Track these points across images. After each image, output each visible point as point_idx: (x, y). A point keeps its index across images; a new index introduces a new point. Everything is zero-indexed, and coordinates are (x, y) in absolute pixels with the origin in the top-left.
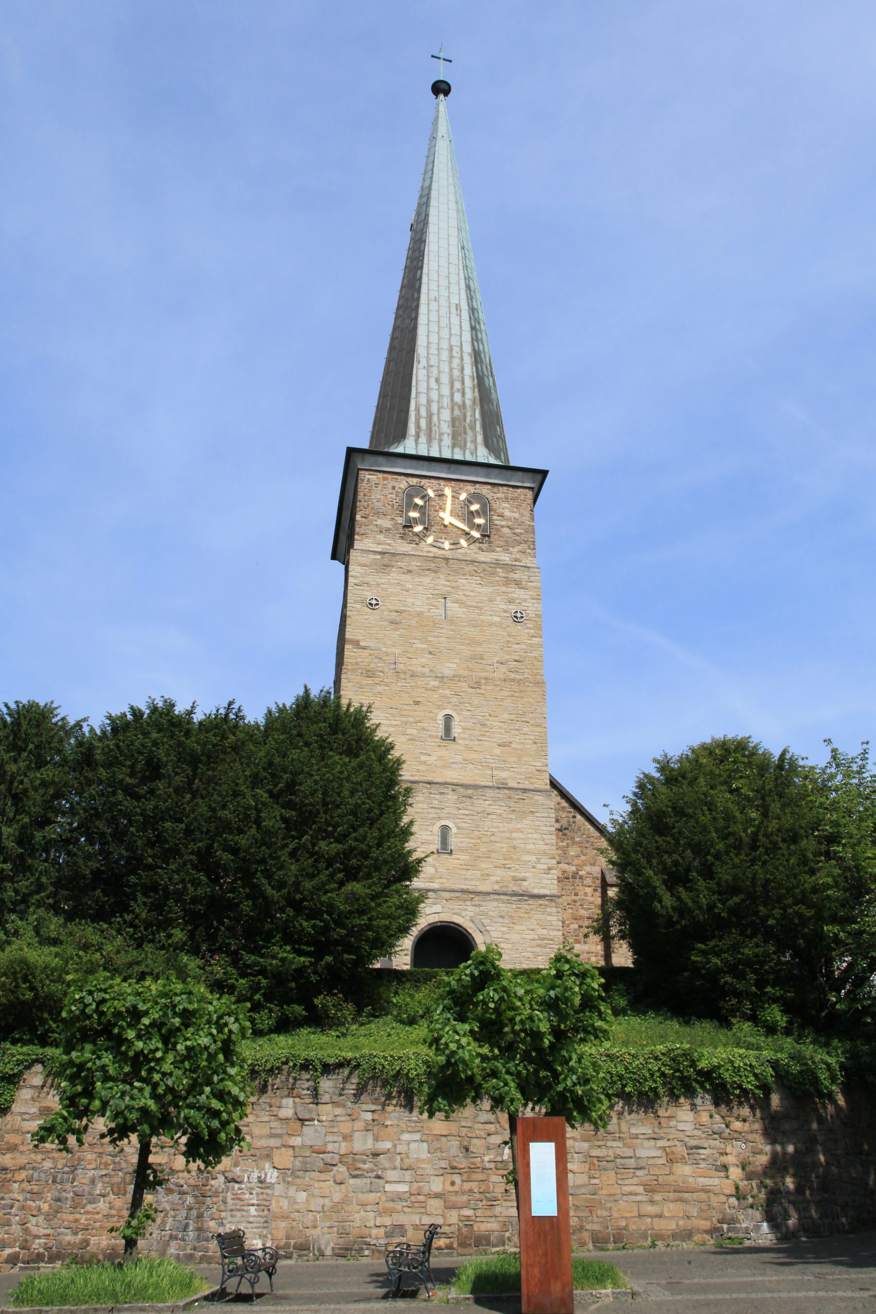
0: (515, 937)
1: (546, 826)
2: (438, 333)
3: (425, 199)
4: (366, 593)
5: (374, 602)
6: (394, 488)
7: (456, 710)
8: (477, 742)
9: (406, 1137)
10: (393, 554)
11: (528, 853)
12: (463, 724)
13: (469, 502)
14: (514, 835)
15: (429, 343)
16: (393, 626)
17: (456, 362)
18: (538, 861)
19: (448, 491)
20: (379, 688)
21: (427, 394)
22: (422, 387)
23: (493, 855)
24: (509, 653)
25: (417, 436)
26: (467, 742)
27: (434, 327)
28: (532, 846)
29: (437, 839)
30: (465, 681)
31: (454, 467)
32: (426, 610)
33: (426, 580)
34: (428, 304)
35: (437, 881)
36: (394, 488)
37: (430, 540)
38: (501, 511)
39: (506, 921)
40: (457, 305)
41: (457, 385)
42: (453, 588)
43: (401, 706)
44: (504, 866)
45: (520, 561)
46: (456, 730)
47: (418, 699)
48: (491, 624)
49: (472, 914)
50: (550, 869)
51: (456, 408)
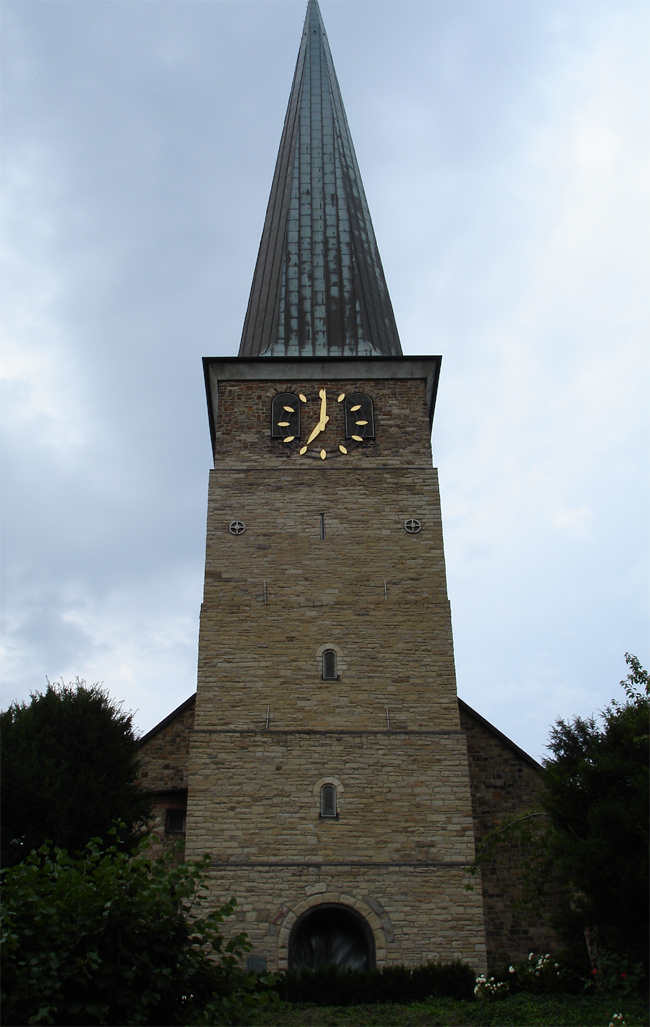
0: (423, 919)
1: (458, 776)
4: (228, 518)
6: (259, 397)
7: (339, 644)
8: (366, 680)
12: (348, 659)
13: (348, 403)
14: (418, 790)
15: (300, 238)
16: (261, 553)
17: (332, 254)
18: (449, 821)
19: (323, 394)
20: (245, 626)
21: (299, 292)
23: (391, 817)
26: (354, 681)
28: (441, 803)
29: (318, 801)
30: (350, 608)
31: (328, 366)
32: (300, 530)
33: (300, 496)
35: (322, 853)
36: (259, 397)
37: (303, 450)
38: (389, 409)
39: (411, 899)
40: (332, 195)
41: (334, 278)
42: (332, 501)
43: (271, 644)
44: (405, 830)
45: (413, 464)
46: (340, 668)
47: (292, 634)
49: (365, 892)
50: (465, 830)
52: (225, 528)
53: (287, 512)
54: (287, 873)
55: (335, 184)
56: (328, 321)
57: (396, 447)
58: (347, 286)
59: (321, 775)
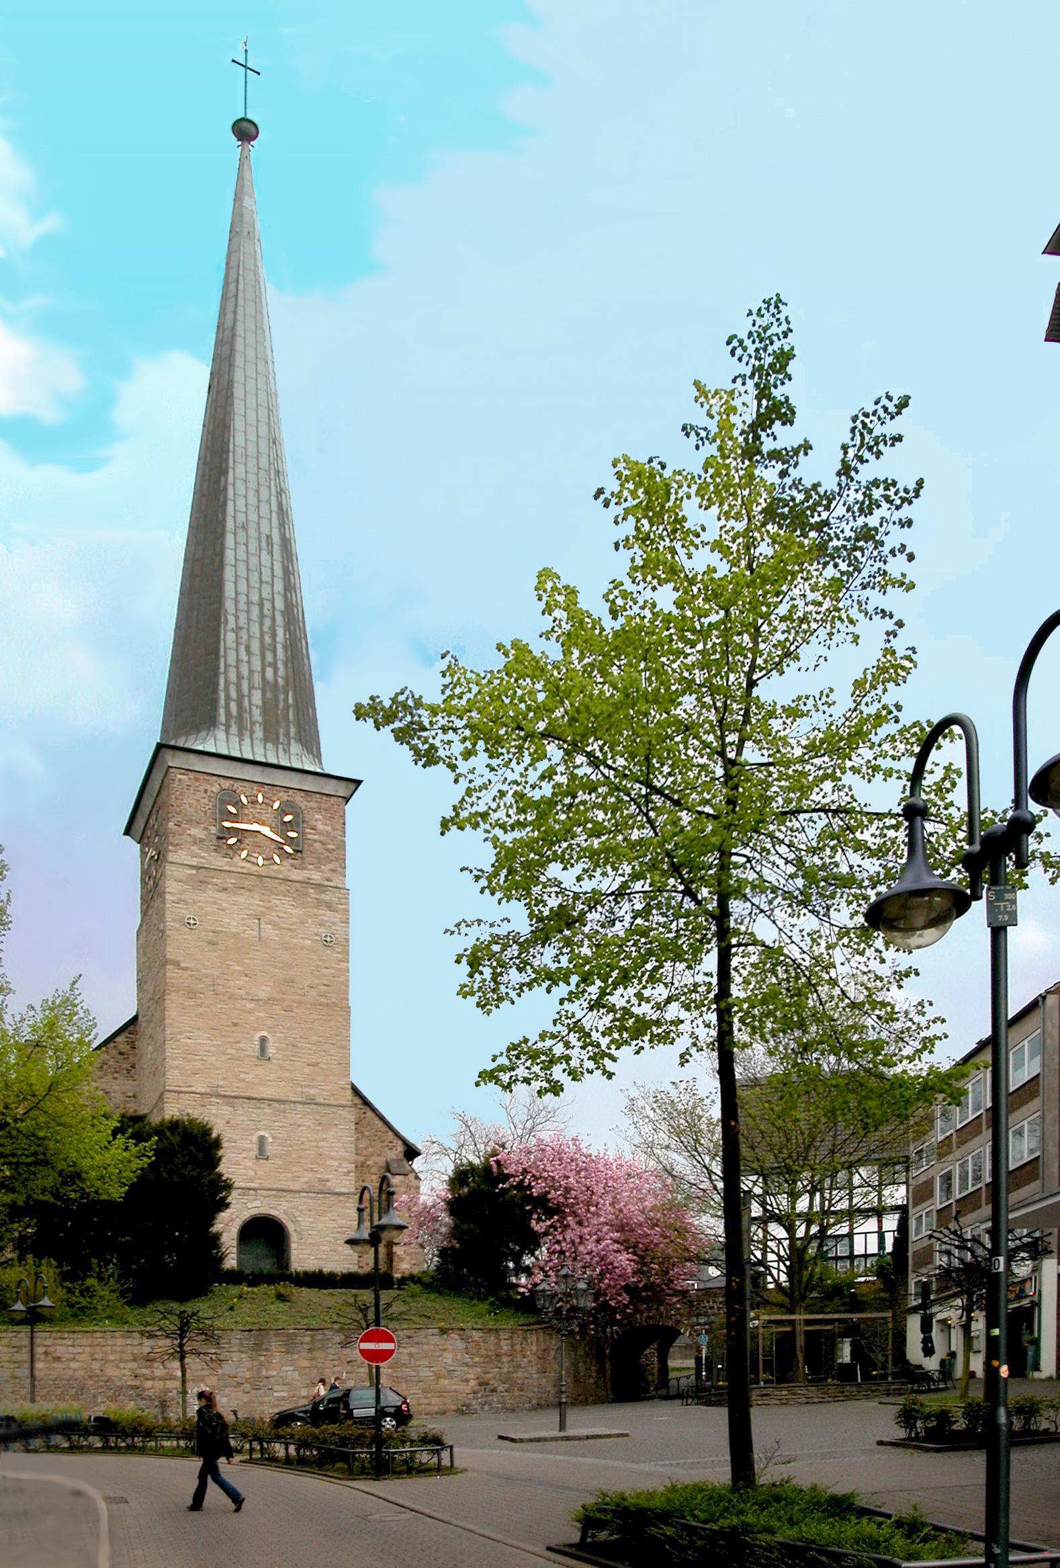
0: (321, 1226)
2: (247, 579)
3: (226, 349)
5: (192, 921)
6: (206, 791)
9: (285, 1368)
11: (332, 1158)
13: (283, 811)
14: (321, 1144)
15: (237, 593)
18: (340, 1166)
20: (201, 1010)
21: (237, 667)
22: (232, 659)
25: (228, 727)
29: (256, 1147)
31: (268, 770)
33: (241, 899)
34: (235, 534)
36: (206, 791)
37: (244, 854)
41: (269, 657)
46: (271, 1051)
51: (268, 688)
55: (270, 519)
56: (266, 708)
57: (319, 863)
58: (281, 672)
59: (258, 1129)
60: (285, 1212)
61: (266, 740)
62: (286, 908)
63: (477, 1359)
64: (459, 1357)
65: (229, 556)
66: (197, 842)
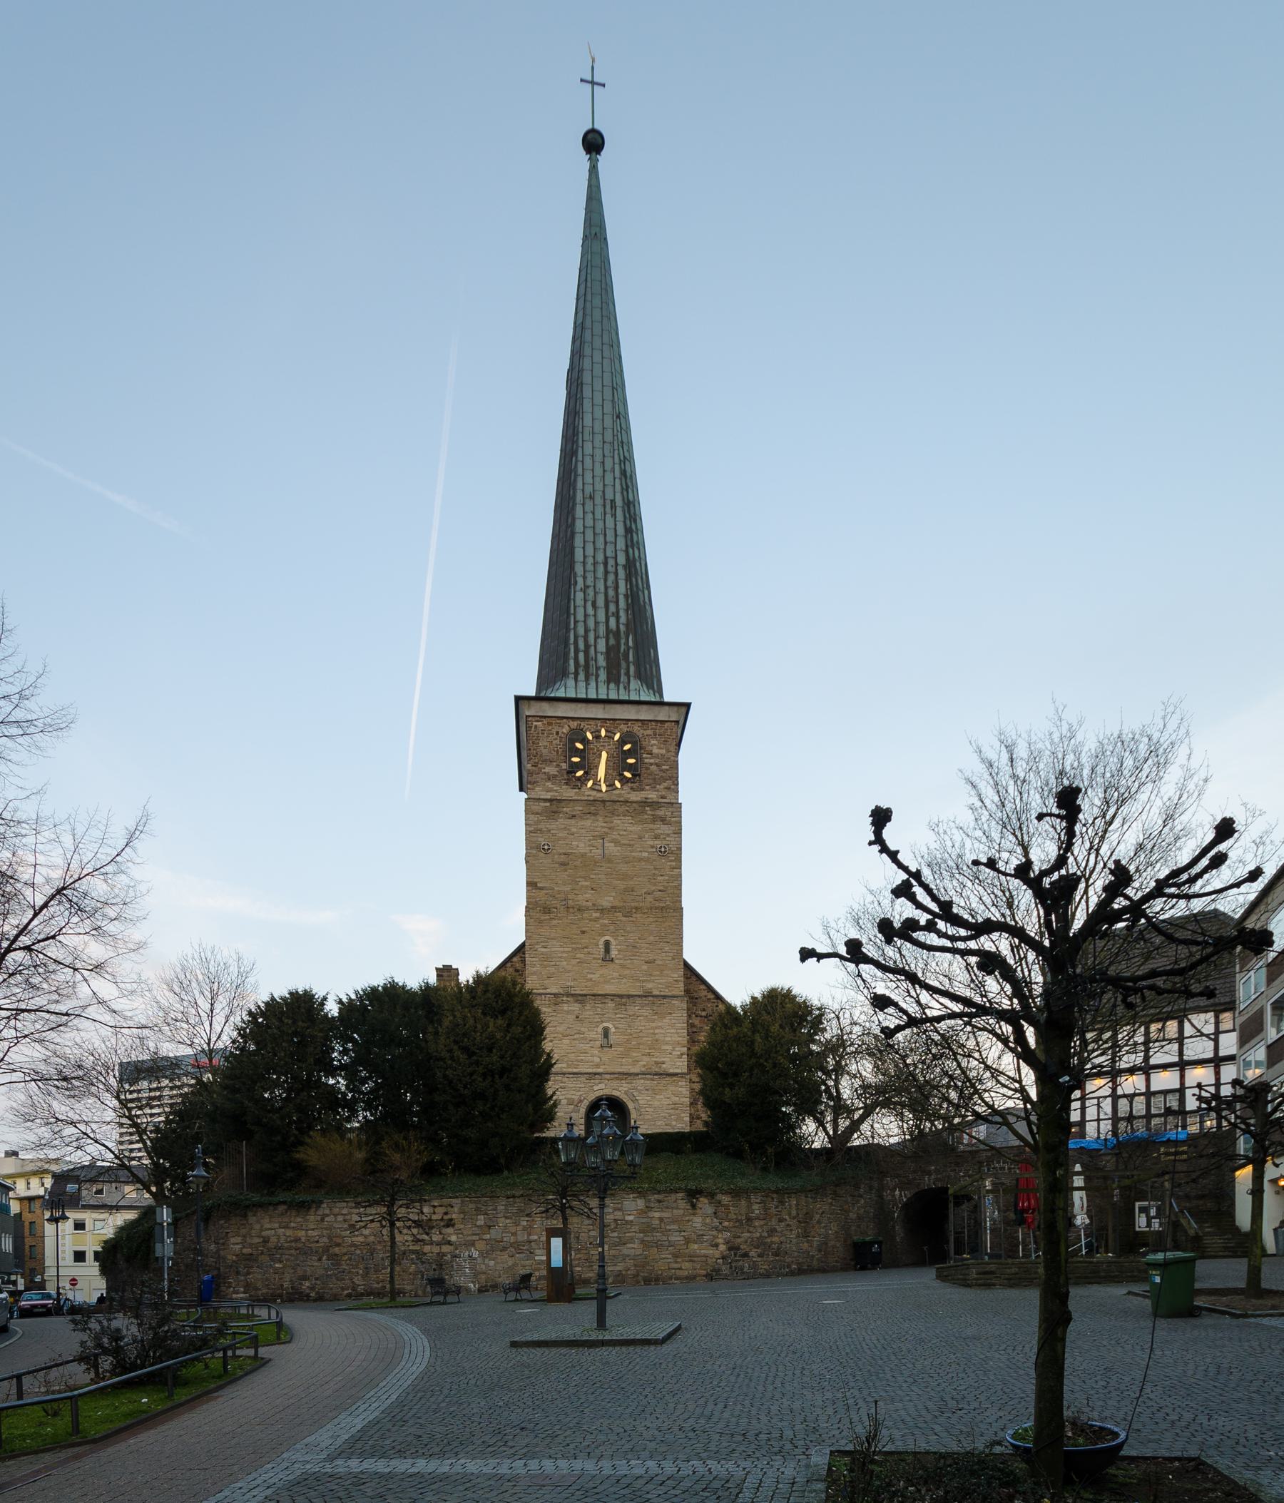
0: (657, 1103)
10: (559, 801)
13: (623, 741)
15: (585, 557)
17: (611, 578)
20: (554, 922)
22: (580, 616)
24: (655, 884)
25: (576, 674)
27: (589, 536)
29: (600, 1037)
31: (608, 707)
33: (588, 823)
37: (590, 784)
41: (612, 608)
46: (614, 953)
48: (641, 860)
52: (538, 848)
53: (580, 836)
54: (583, 1079)
58: (623, 619)
60: (626, 1093)
61: (608, 681)
62: (626, 825)
63: (726, 1224)
64: (708, 1220)
65: (579, 525)
66: (550, 778)
